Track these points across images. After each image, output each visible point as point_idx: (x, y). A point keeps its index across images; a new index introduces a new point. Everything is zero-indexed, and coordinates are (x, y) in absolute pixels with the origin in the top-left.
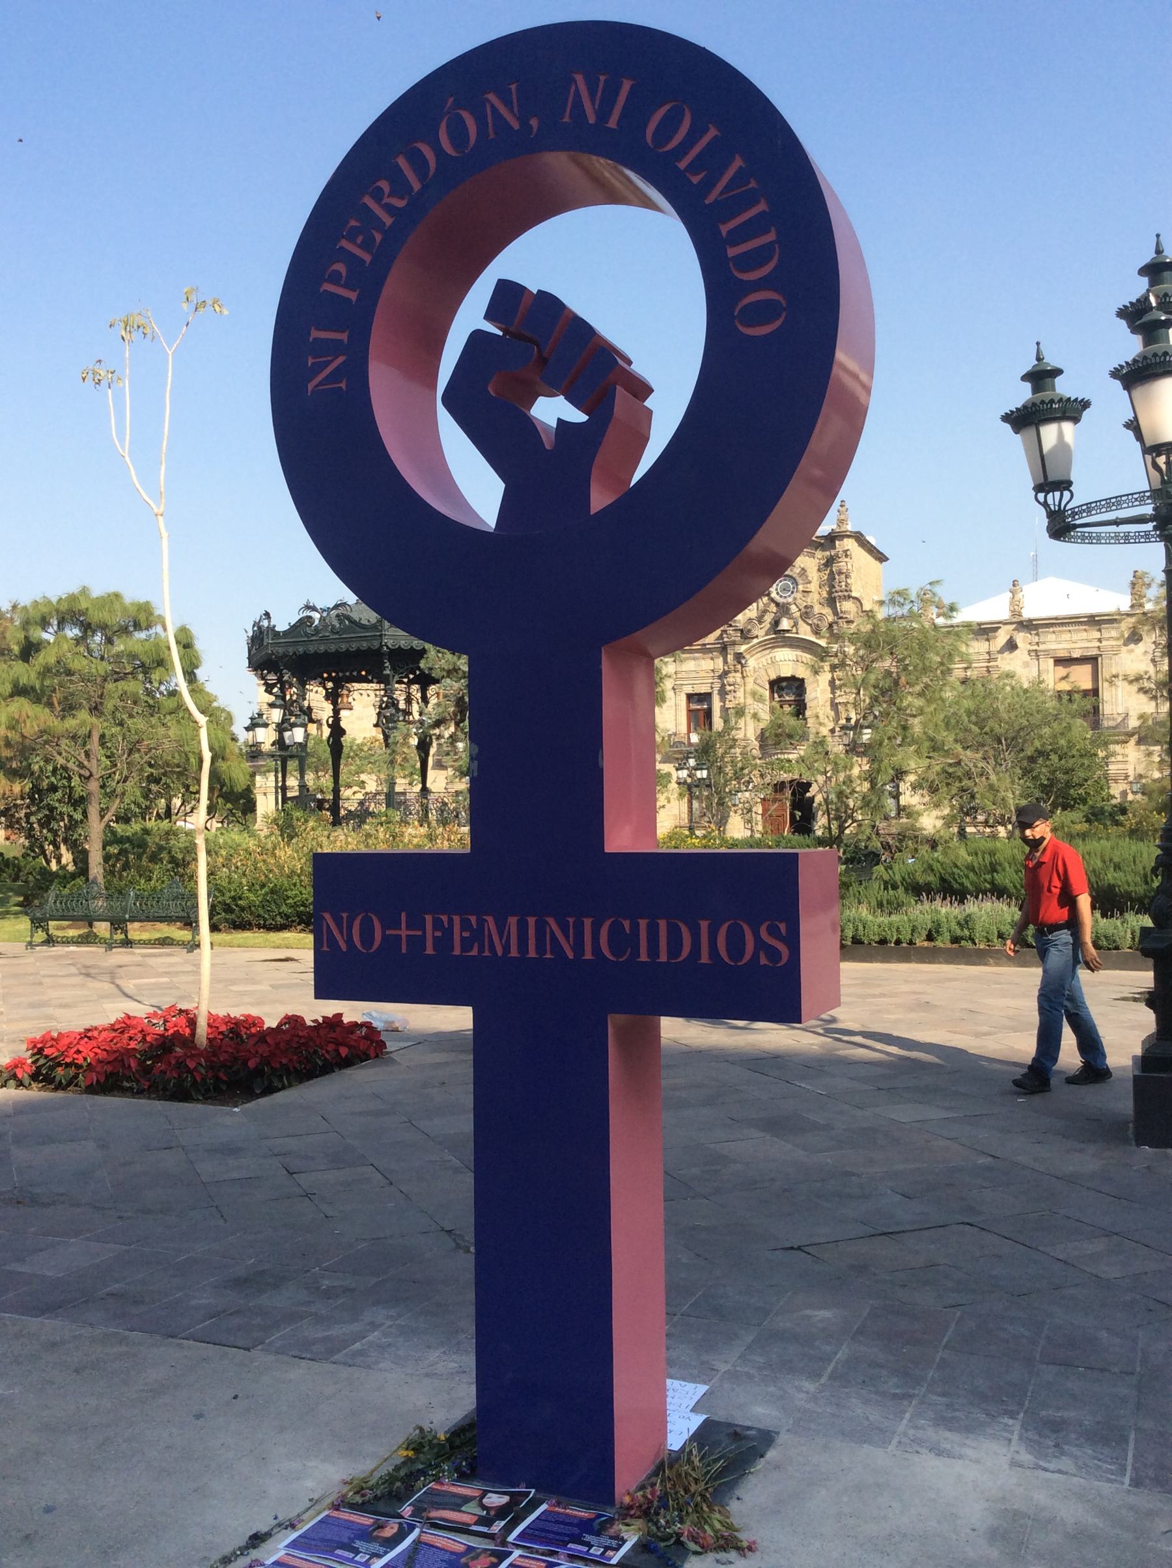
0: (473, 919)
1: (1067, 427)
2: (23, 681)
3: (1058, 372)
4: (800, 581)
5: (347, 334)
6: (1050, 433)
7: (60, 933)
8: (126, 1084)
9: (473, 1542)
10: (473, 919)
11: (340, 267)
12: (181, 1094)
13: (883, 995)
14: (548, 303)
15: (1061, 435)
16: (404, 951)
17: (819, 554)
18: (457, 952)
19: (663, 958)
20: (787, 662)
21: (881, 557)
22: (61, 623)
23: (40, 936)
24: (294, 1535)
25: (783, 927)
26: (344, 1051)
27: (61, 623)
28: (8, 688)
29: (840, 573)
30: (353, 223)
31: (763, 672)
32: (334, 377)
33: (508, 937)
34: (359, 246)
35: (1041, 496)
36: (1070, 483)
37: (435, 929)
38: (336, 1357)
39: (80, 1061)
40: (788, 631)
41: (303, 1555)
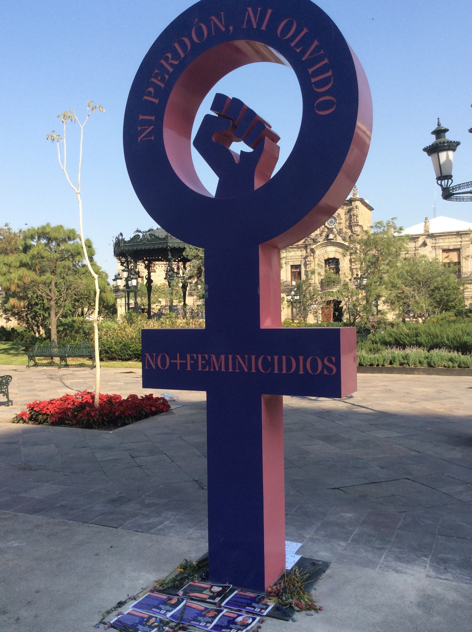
0: (206, 356)
1: (450, 153)
2: (24, 261)
3: (446, 130)
4: (337, 219)
5: (154, 117)
6: (443, 156)
7: (40, 362)
8: (67, 422)
9: (207, 606)
10: (206, 356)
11: (151, 89)
12: (89, 426)
13: (371, 387)
14: (237, 103)
15: (448, 156)
16: (178, 369)
17: (345, 207)
18: (200, 369)
19: (284, 371)
20: (332, 252)
21: (371, 209)
22: (39, 238)
23: (32, 363)
24: (136, 602)
25: (334, 359)
26: (154, 409)
27: (39, 238)
28: (18, 264)
29: (354, 215)
30: (156, 71)
31: (322, 256)
32: (149, 135)
33: (221, 363)
34: (159, 81)
35: (439, 182)
36: (451, 176)
37: (191, 360)
38: (152, 531)
39: (48, 413)
40: (332, 239)
41: (139, 610)
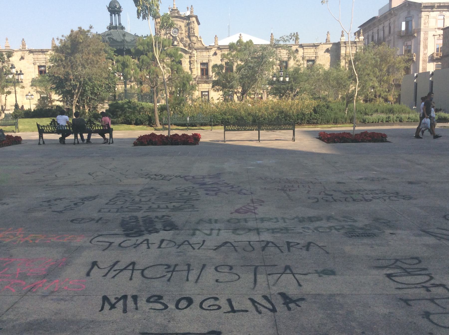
17: (185, 21)
29: (192, 28)
